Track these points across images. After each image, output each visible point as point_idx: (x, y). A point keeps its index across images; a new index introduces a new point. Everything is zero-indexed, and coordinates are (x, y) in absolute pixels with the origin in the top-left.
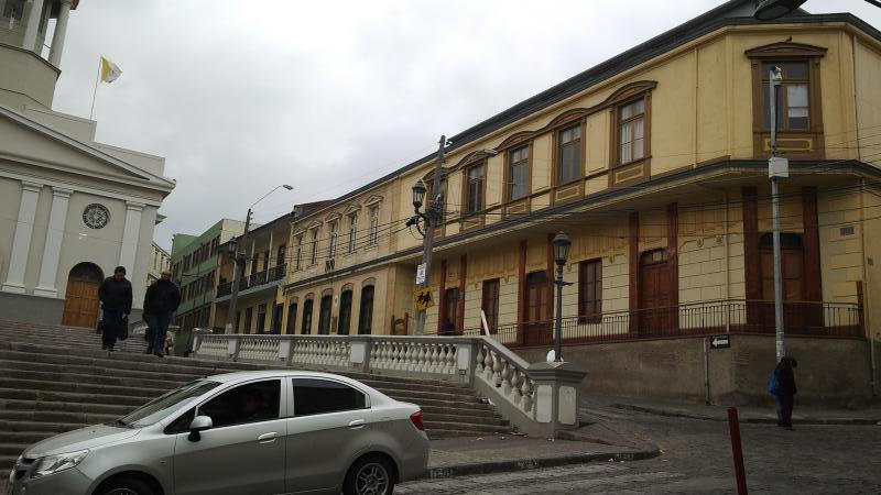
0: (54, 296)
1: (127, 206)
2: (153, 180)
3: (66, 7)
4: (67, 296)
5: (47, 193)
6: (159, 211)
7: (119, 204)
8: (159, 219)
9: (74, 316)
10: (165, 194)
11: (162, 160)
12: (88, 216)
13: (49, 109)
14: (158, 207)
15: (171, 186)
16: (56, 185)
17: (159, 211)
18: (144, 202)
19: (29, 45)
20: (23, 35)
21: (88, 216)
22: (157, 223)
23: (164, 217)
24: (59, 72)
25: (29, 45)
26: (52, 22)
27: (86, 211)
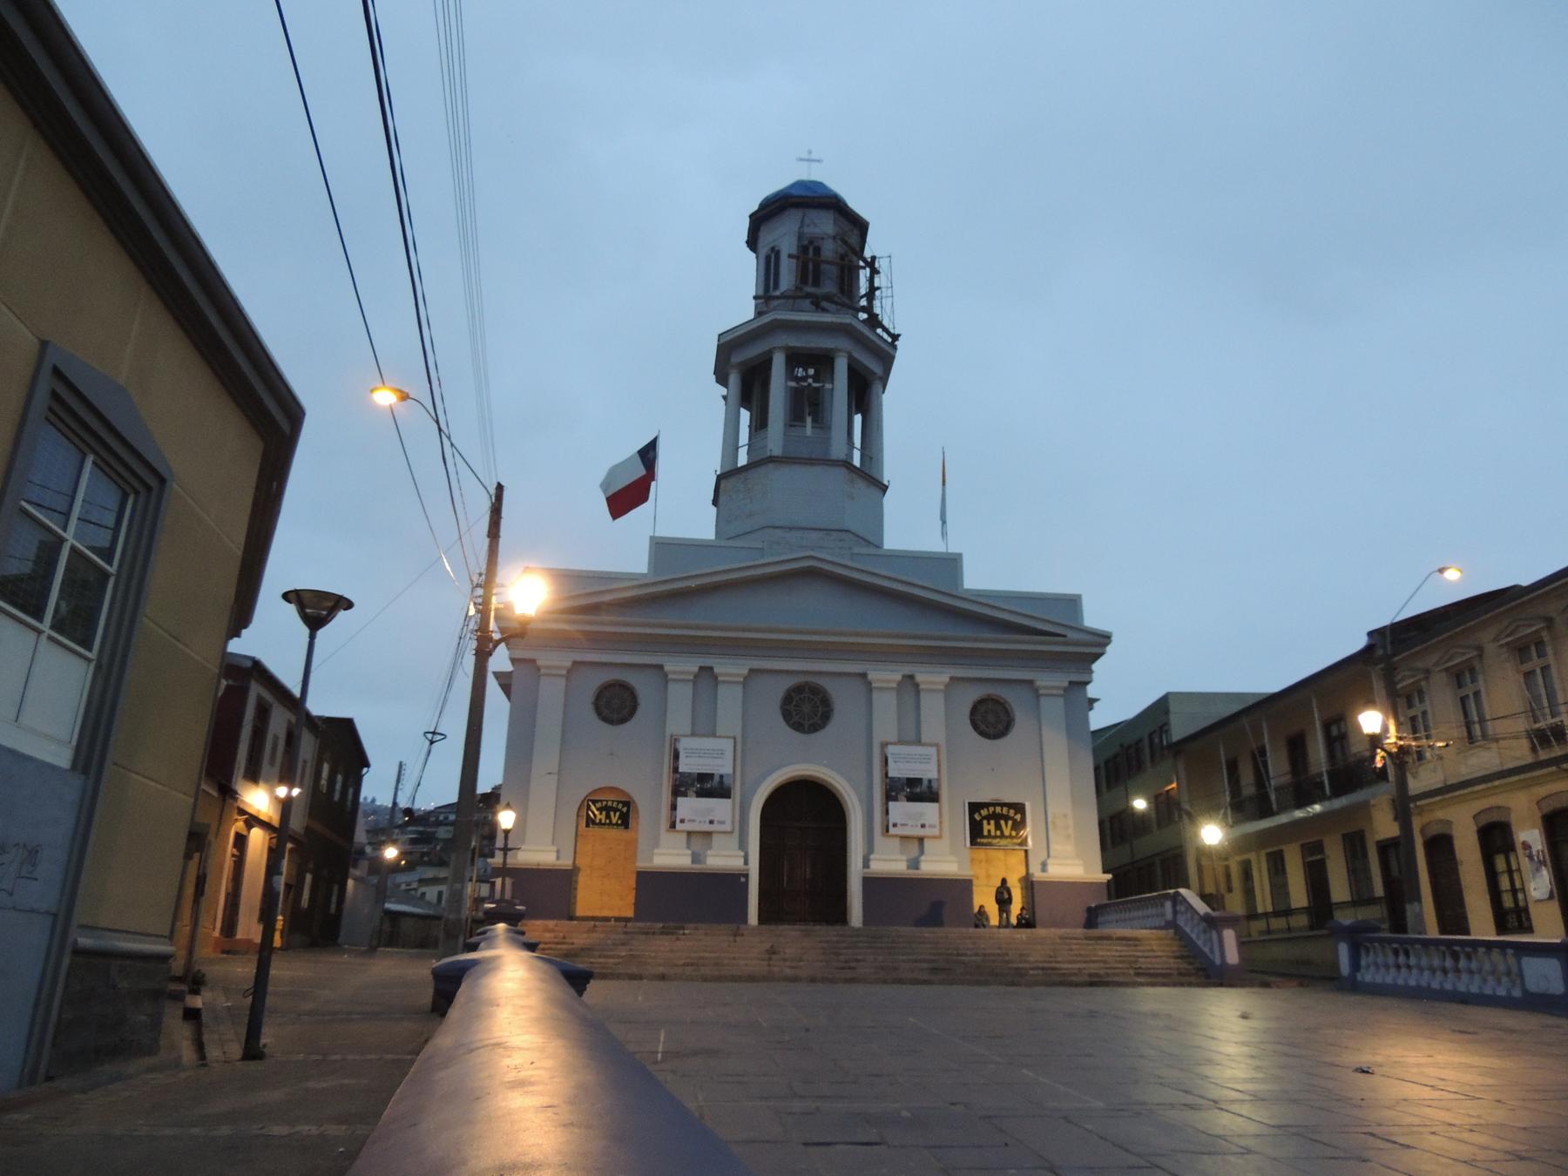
2: (1071, 635)
3: (877, 386)
6: (1091, 691)
8: (1092, 701)
13: (879, 546)
14: (1087, 683)
19: (837, 451)
20: (826, 442)
24: (884, 489)
25: (837, 451)
26: (858, 419)
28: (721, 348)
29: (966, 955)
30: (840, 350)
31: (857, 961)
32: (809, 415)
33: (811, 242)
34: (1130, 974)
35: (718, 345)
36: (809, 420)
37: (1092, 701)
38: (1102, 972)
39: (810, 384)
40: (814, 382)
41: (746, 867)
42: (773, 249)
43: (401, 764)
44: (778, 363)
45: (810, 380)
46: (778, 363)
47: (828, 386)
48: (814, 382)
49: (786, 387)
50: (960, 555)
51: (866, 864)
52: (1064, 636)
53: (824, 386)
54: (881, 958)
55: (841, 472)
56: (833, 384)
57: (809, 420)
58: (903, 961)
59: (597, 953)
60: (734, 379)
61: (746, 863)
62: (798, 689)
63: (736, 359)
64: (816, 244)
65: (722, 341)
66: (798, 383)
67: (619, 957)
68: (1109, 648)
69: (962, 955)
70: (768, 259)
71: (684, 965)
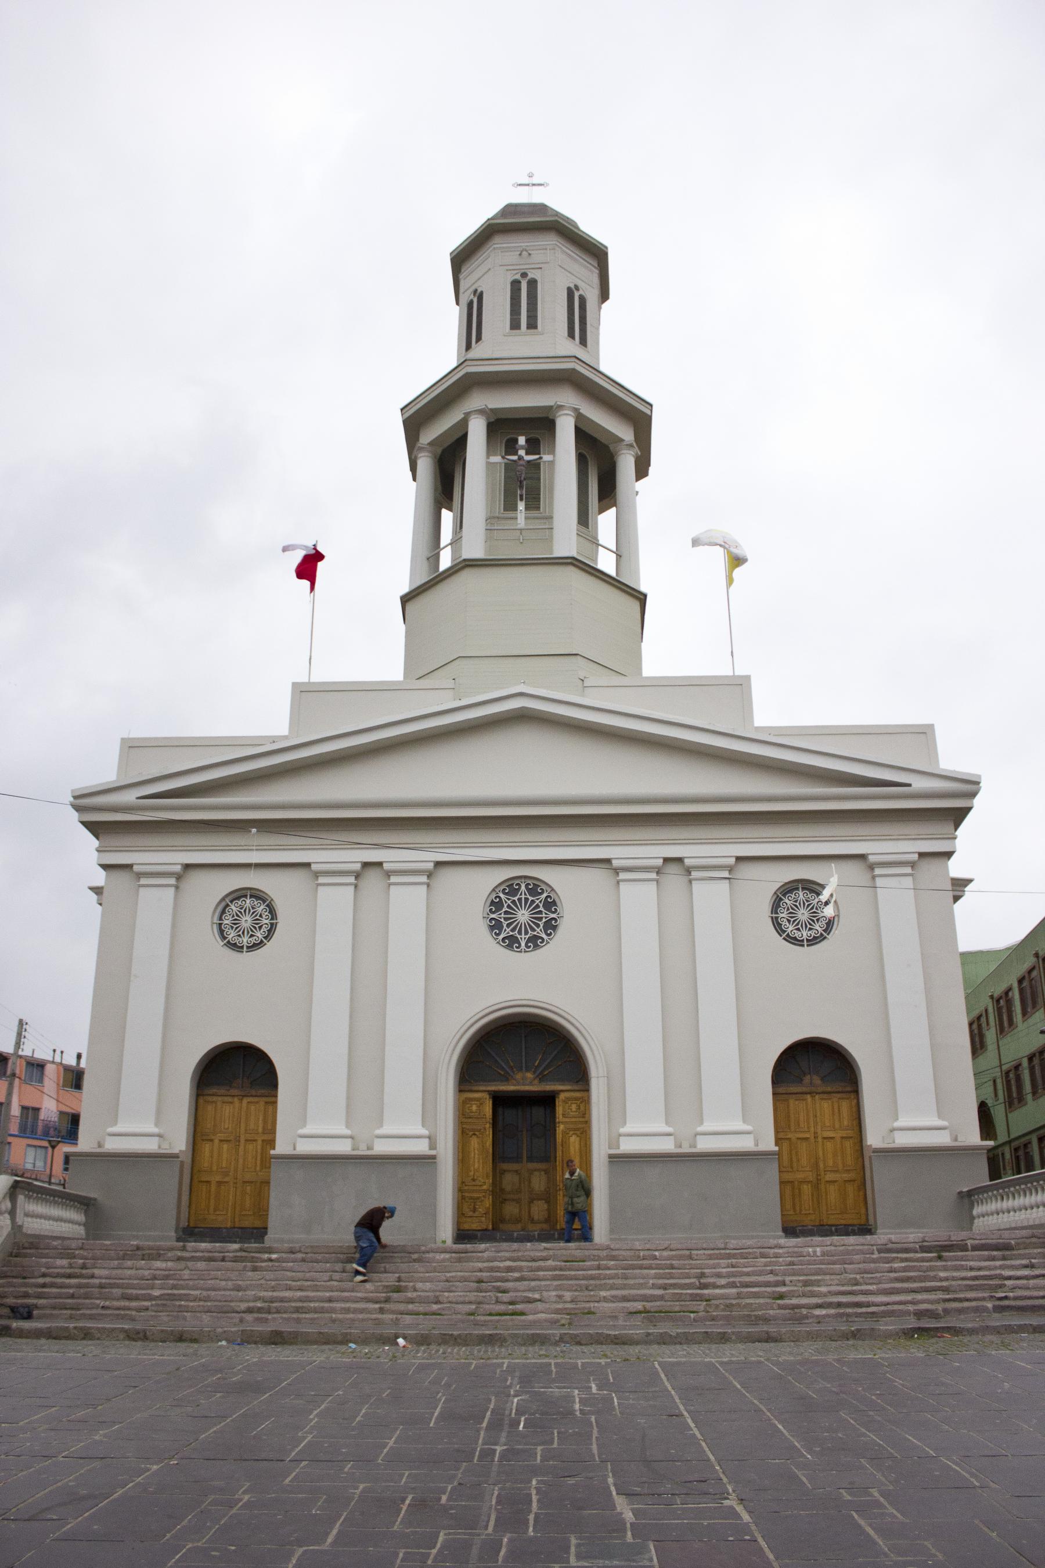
0: (746, 1144)
1: (872, 867)
2: (919, 784)
4: (778, 1141)
5: (674, 879)
6: (956, 868)
7: (854, 872)
8: (960, 886)
9: (806, 1189)
10: (958, 816)
11: (924, 733)
12: (783, 915)
14: (949, 855)
15: (970, 787)
16: (691, 852)
17: (956, 868)
18: (910, 848)
21: (783, 915)
22: (956, 899)
23: (968, 882)
27: (776, 906)
28: (406, 423)
29: (715, 1286)
30: (560, 407)
31: (530, 1301)
32: (521, 500)
33: (524, 275)
34: (985, 1309)
35: (405, 422)
36: (521, 506)
37: (960, 886)
38: (940, 1307)
39: (521, 458)
40: (527, 454)
41: (433, 1152)
42: (475, 291)
43: (21, 1023)
44: (477, 433)
45: (522, 452)
46: (477, 433)
47: (546, 458)
48: (527, 454)
49: (488, 464)
50: (748, 678)
51: (614, 1142)
52: (909, 785)
53: (541, 458)
54: (568, 1295)
55: (574, 577)
56: (554, 456)
57: (521, 506)
58: (605, 1299)
59: (116, 1292)
60: (425, 464)
61: (433, 1146)
62: (511, 887)
63: (430, 435)
64: (530, 276)
65: (407, 415)
66: (503, 458)
67: (150, 1298)
68: (977, 802)
69: (705, 1286)
70: (470, 305)
71: (249, 1311)
